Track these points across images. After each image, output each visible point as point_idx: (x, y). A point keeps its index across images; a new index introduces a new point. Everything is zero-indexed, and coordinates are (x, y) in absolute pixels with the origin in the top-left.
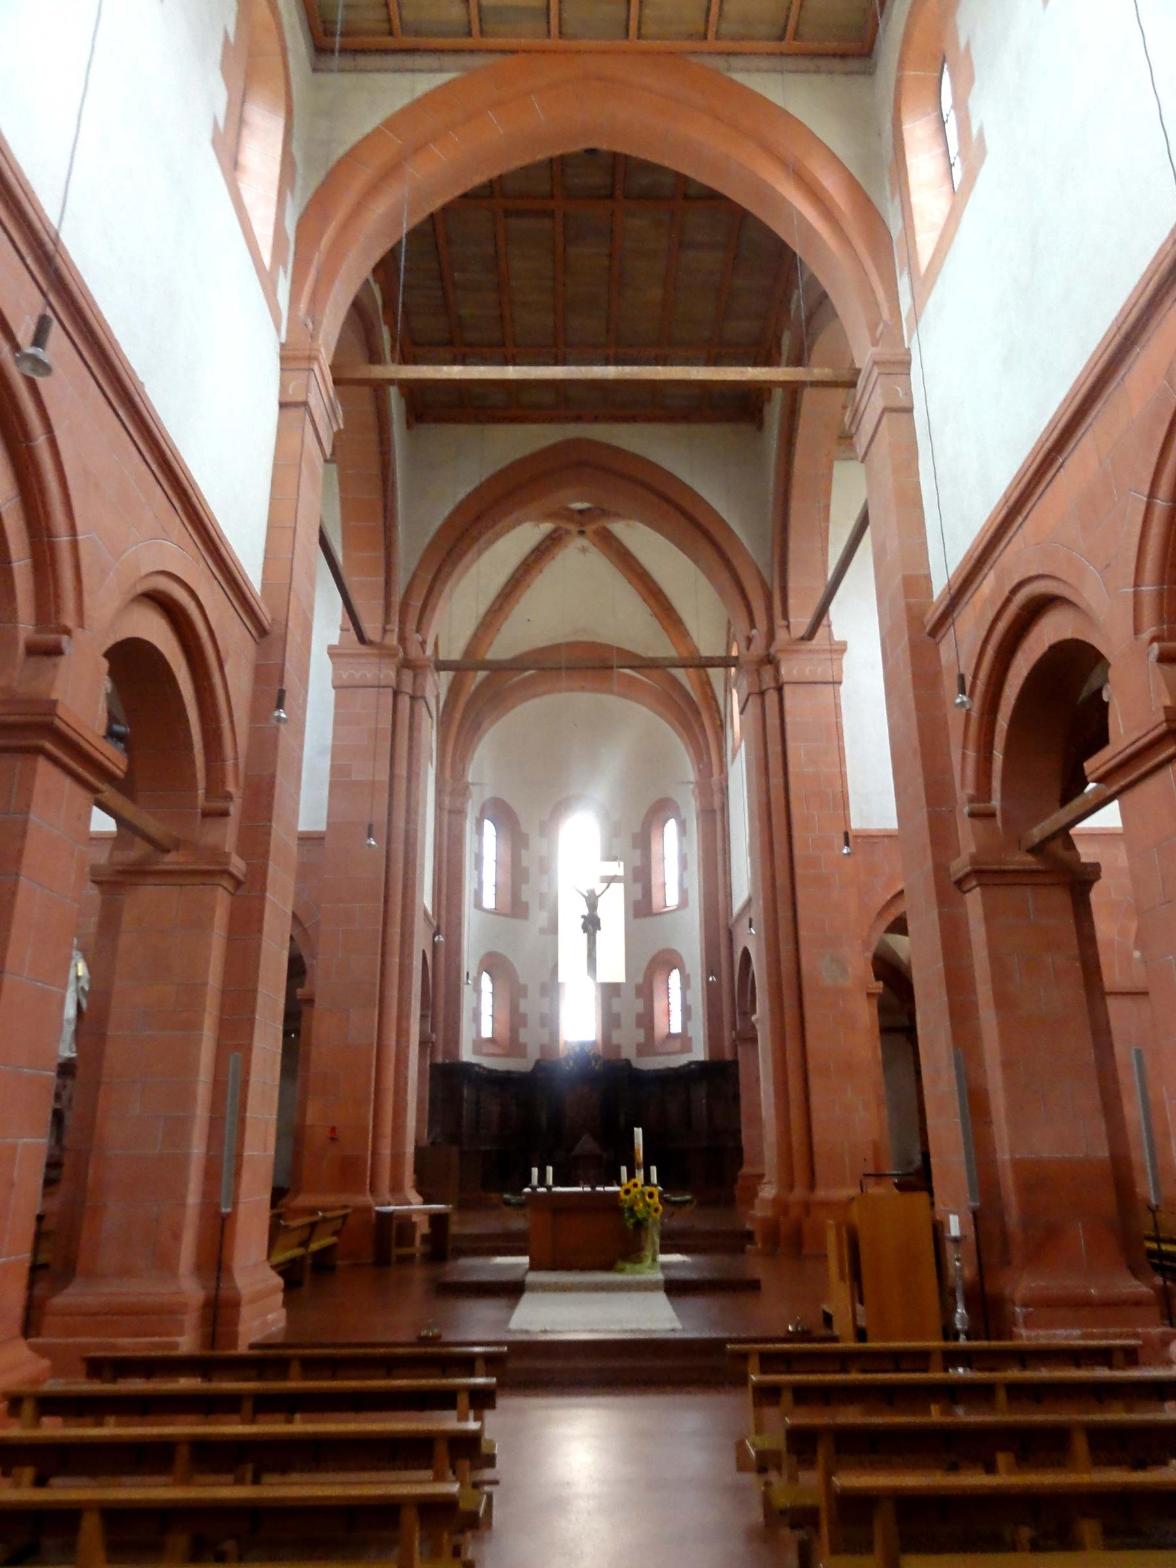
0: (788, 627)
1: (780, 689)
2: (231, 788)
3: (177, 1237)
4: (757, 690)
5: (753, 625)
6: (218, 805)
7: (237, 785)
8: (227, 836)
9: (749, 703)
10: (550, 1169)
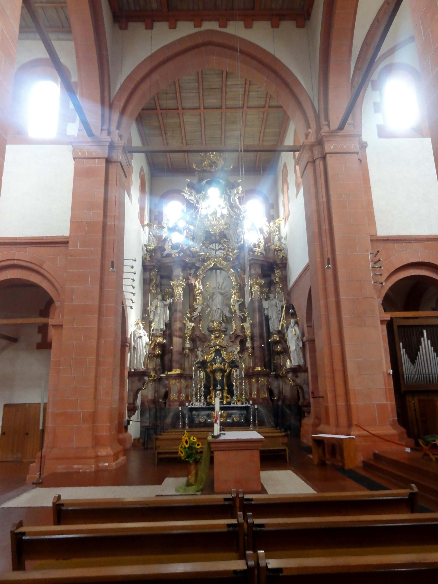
0: (328, 125)
1: (324, 158)
4: (311, 160)
5: (309, 127)
9: (308, 166)
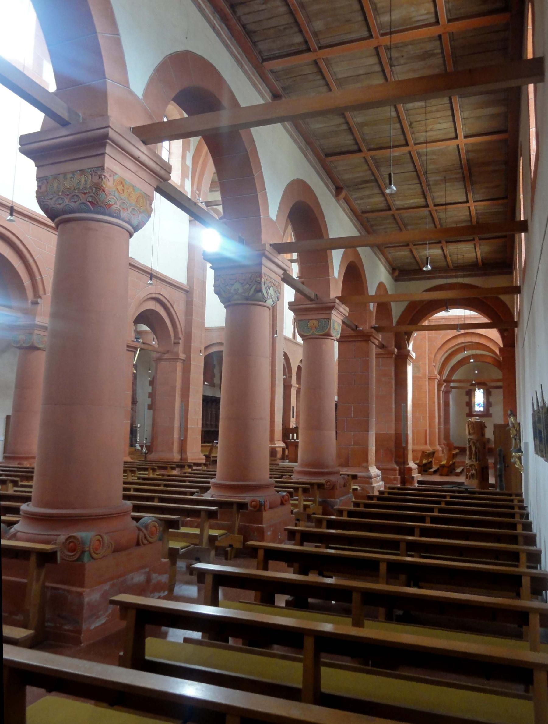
2: (180, 336)
3: (173, 444)
6: (176, 341)
7: (182, 334)
8: (180, 349)
10: (295, 435)
